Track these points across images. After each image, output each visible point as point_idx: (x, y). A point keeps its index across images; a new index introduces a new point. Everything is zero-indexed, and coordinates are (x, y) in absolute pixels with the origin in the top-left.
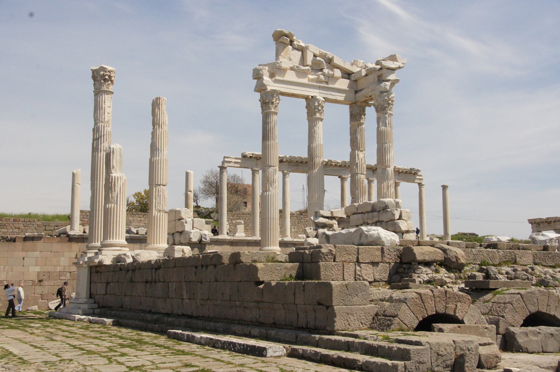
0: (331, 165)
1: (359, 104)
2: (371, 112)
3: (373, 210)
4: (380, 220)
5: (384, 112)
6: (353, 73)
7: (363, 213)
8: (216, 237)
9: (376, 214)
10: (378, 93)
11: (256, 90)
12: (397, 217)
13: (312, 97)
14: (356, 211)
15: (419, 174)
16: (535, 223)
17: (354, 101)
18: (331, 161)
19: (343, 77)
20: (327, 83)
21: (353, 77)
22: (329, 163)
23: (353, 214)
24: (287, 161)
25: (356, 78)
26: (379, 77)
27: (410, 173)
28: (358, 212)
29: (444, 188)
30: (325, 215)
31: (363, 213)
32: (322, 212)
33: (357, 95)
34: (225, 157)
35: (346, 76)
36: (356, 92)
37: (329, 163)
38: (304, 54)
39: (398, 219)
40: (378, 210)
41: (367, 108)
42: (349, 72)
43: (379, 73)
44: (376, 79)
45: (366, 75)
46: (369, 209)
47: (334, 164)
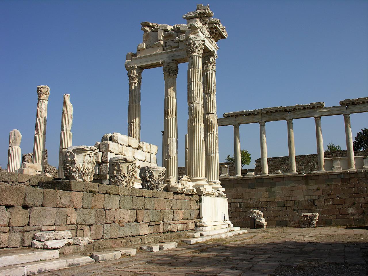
37: (297, 108)
47: (302, 108)
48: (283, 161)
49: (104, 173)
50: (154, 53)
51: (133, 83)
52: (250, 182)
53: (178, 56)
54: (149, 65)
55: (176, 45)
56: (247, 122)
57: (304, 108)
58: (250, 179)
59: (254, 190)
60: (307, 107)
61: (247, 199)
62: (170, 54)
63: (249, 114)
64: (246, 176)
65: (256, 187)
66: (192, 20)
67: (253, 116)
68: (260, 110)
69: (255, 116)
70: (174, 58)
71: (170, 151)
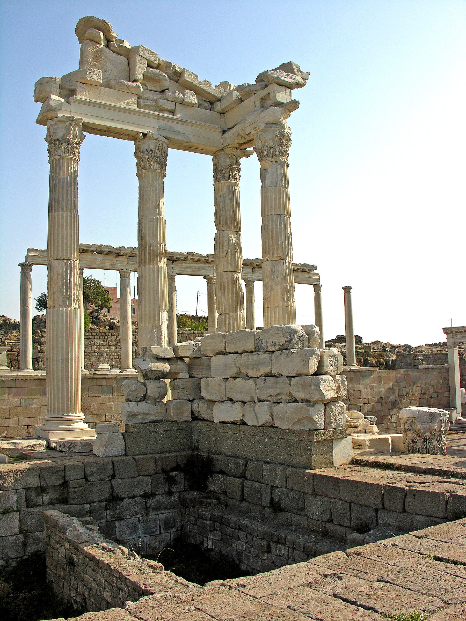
0: (193, 260)
1: (228, 151)
2: (250, 168)
3: (258, 350)
4: (274, 372)
5: (274, 159)
6: (219, 100)
7: (237, 353)
8: (14, 374)
9: (264, 356)
10: (262, 126)
11: (41, 121)
12: (313, 368)
13: (145, 135)
14: (222, 348)
15: (315, 271)
16: (451, 332)
17: (220, 147)
18: (192, 254)
19: (200, 106)
20: (173, 113)
21: (218, 107)
22: (190, 258)
23: (218, 354)
24: (125, 255)
25: (223, 107)
26: (263, 99)
27: (303, 271)
28: (228, 350)
29: (347, 290)
30: (163, 355)
31: (237, 353)
32: (155, 350)
33: (227, 135)
34: (29, 250)
35: (206, 104)
36: (224, 131)
37: (190, 258)
38: (131, 62)
39: (316, 374)
40: (270, 349)
41: (243, 160)
42: (213, 99)
43: (263, 93)
44: (258, 104)
45: (241, 100)
46: (251, 346)
47: (196, 258)
48: (92, 337)
49: (338, 426)
50: (116, 105)
51: (71, 159)
52: (104, 383)
53: (179, 133)
54: (108, 128)
55: (171, 106)
56: (102, 266)
57: (199, 260)
58: (106, 378)
59: (112, 398)
60: (203, 259)
61: (99, 416)
62: (162, 123)
63: (110, 253)
64: (97, 373)
65: (115, 394)
66: (283, 88)
67: (112, 257)
68: (131, 250)
69: (117, 259)
70: (170, 136)
71: (163, 340)
